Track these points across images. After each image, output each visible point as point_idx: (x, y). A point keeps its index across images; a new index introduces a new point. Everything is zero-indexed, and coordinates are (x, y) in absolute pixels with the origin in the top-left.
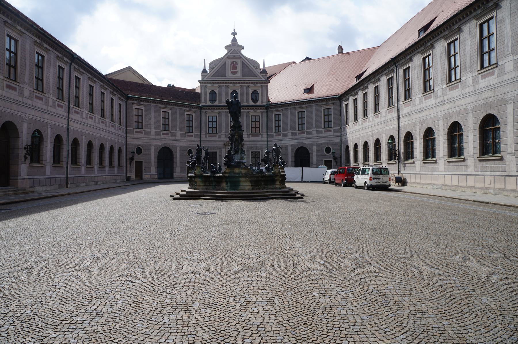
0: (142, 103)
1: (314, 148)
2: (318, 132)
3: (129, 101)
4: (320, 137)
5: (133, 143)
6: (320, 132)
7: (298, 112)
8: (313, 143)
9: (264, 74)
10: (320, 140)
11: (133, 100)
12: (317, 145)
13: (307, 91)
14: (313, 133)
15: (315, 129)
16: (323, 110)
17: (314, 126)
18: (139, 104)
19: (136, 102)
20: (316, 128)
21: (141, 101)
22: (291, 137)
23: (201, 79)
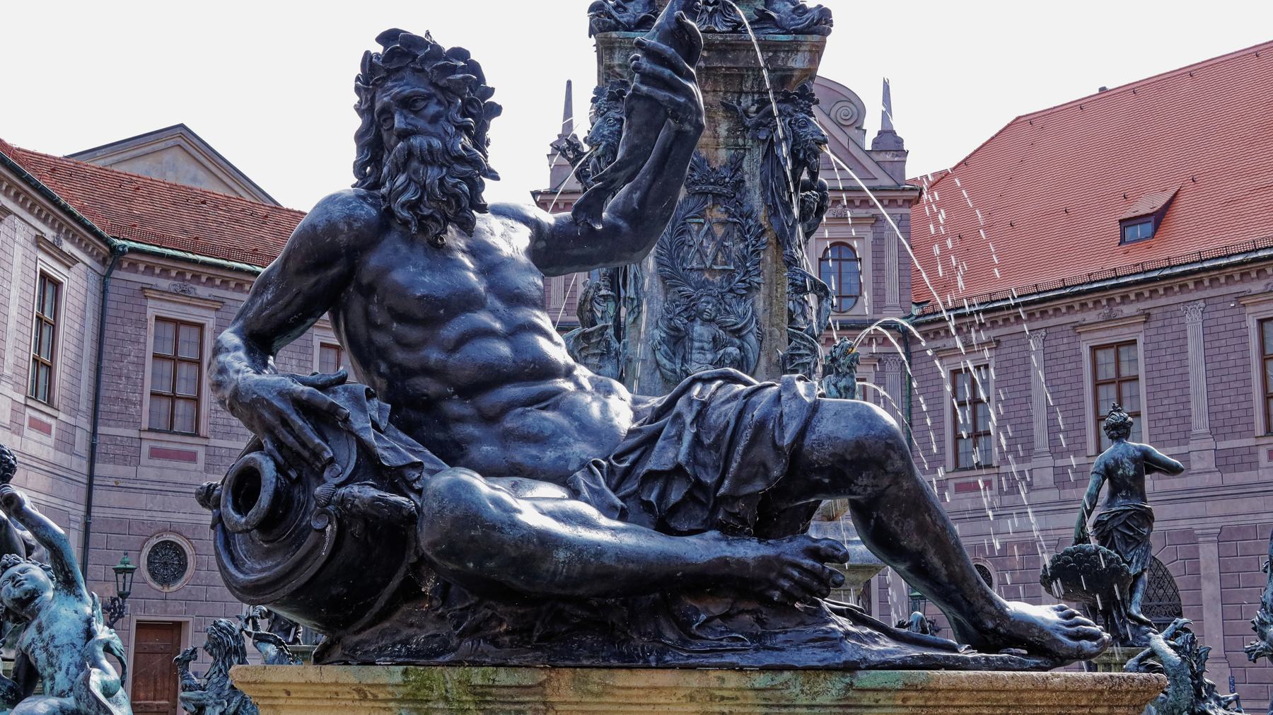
0: (202, 291)
1: (1208, 553)
2: (1225, 461)
3: (115, 273)
4: (1243, 491)
5: (130, 514)
6: (1247, 460)
7: (1094, 349)
8: (1197, 526)
9: (888, 157)
10: (1244, 505)
11: (149, 269)
12: (1223, 537)
13: (1139, 231)
14: (1196, 466)
15: (1210, 443)
16: (1252, 324)
17: (1200, 423)
18: (182, 294)
19: (164, 284)
20: (1215, 433)
21: (196, 277)
22: (1053, 495)
23: (545, 185)
